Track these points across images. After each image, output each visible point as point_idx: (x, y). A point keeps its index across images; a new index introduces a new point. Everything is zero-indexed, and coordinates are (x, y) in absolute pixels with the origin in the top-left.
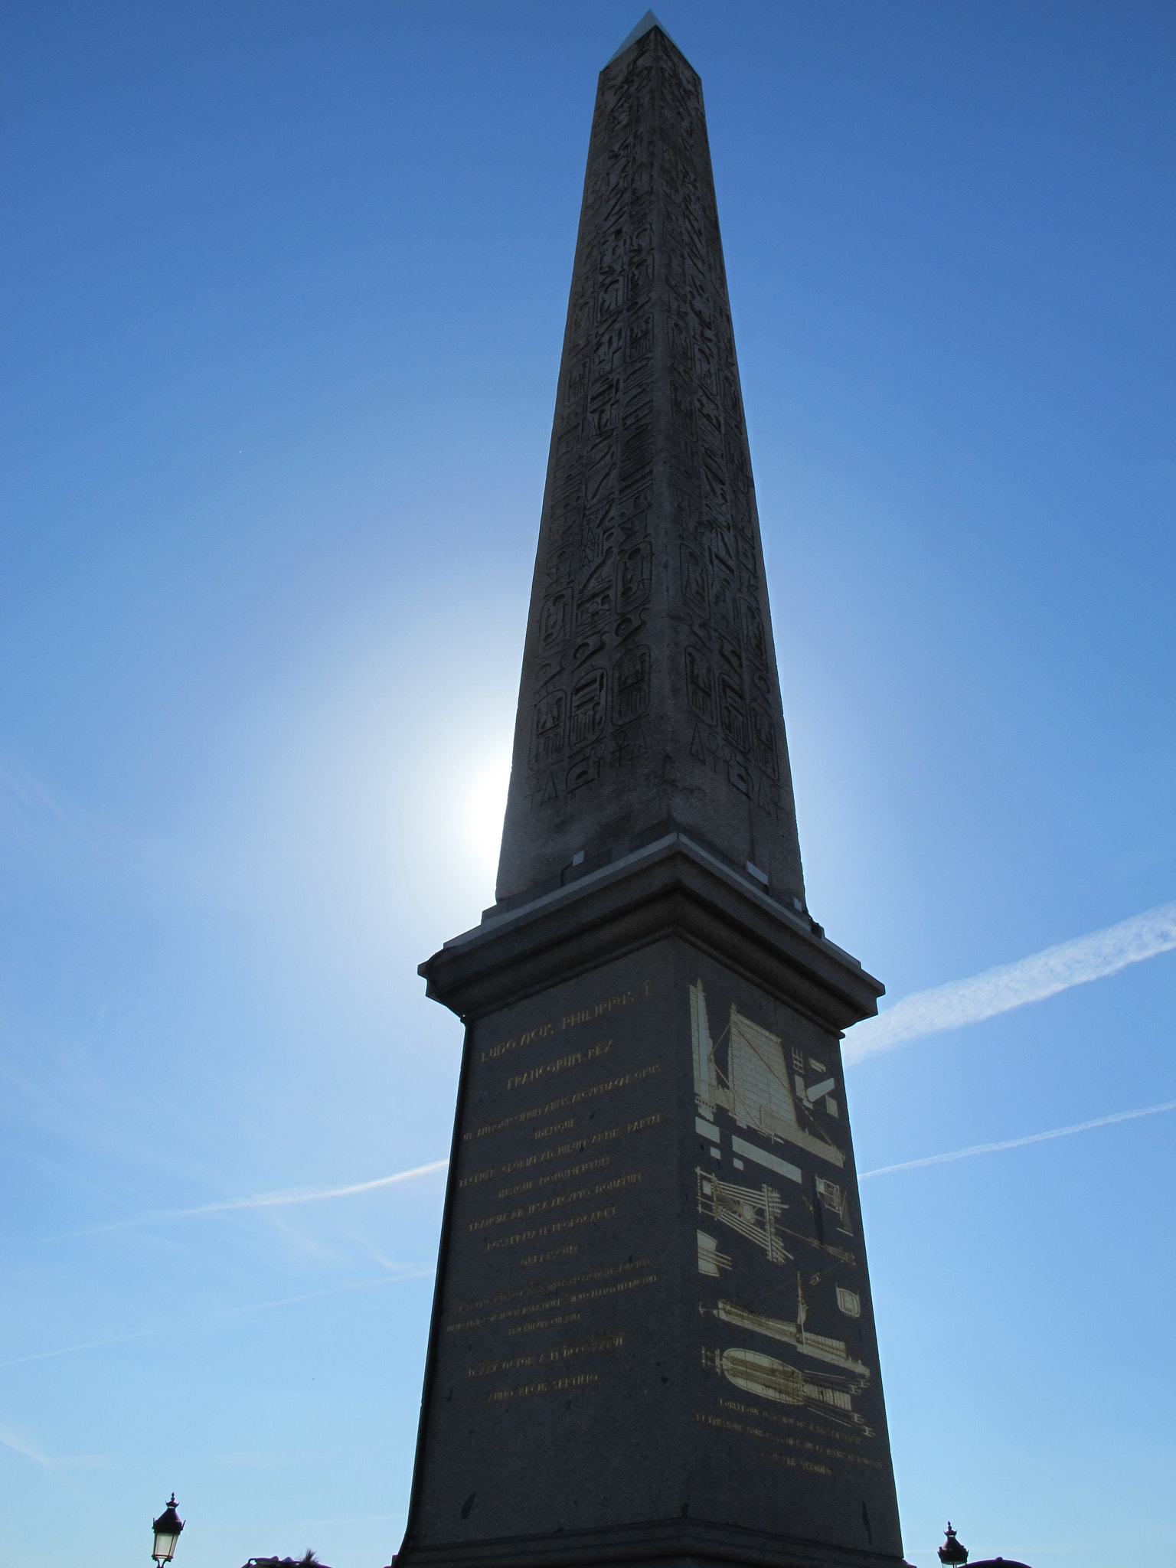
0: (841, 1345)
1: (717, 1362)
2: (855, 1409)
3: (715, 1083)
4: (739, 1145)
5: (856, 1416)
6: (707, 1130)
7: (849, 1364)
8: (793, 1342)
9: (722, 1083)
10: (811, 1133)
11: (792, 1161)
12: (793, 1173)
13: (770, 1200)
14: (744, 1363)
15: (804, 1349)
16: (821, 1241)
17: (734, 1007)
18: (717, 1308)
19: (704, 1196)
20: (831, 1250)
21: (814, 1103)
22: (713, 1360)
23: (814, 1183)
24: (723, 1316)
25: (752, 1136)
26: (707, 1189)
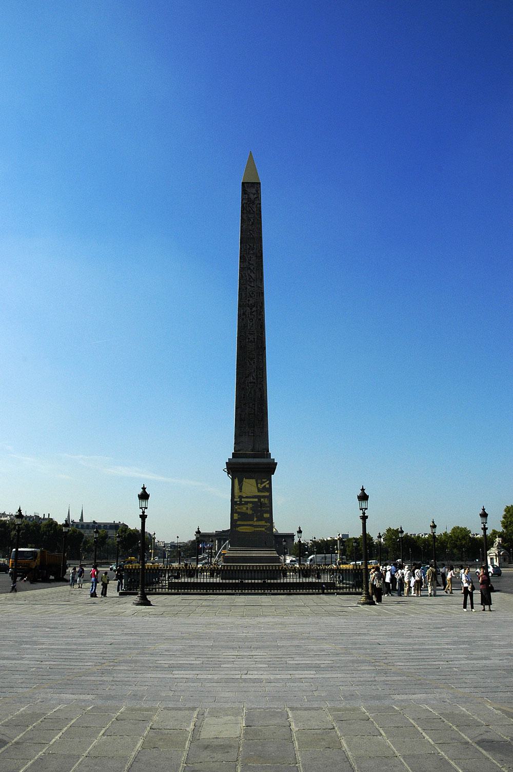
4: (243, 500)
7: (266, 524)
9: (241, 492)
12: (256, 500)
13: (250, 505)
15: (254, 524)
16: (261, 507)
25: (247, 497)
26: (236, 508)
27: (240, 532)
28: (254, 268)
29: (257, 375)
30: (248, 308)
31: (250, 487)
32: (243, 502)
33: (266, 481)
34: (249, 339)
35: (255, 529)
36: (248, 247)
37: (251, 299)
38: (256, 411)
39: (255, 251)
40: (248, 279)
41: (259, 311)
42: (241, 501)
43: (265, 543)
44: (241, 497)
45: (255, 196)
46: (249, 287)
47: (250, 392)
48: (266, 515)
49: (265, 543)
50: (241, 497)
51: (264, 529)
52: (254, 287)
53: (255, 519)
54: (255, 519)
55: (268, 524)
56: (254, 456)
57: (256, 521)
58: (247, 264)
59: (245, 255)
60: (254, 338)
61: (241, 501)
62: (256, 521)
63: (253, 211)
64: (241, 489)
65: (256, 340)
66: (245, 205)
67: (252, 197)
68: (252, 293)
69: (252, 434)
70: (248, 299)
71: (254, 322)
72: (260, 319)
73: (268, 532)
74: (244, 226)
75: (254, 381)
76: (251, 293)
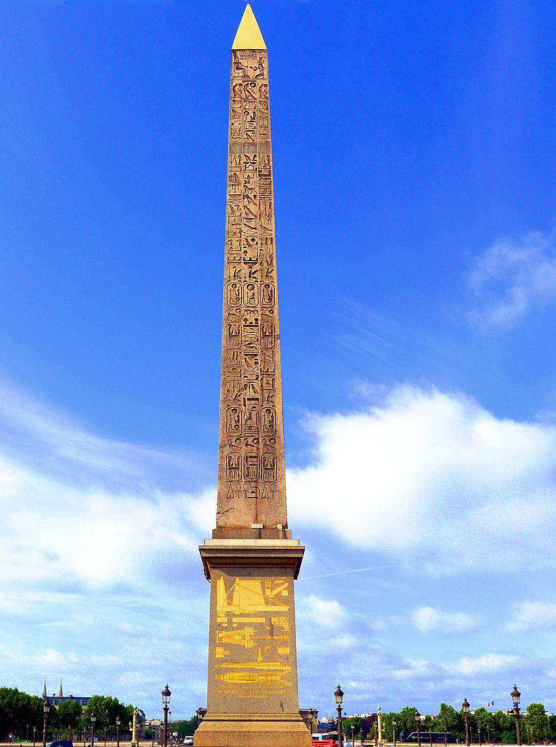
0: (279, 663)
1: (222, 678)
4: (235, 620)
5: (281, 681)
6: (222, 619)
8: (254, 667)
9: (229, 604)
12: (263, 620)
13: (249, 631)
16: (272, 635)
19: (219, 638)
20: (276, 637)
23: (271, 619)
24: (225, 666)
25: (242, 615)
26: (220, 635)
27: (227, 684)
28: (255, 196)
29: (262, 386)
30: (246, 266)
31: (250, 594)
32: (236, 625)
33: (282, 584)
34: (246, 320)
36: (244, 159)
37: (248, 249)
38: (261, 450)
39: (256, 166)
40: (244, 215)
41: (265, 271)
42: (230, 622)
43: (282, 706)
44: (229, 615)
45: (258, 72)
46: (245, 229)
47: (250, 418)
48: (283, 651)
49: (282, 706)
51: (278, 678)
52: (254, 228)
53: (260, 658)
54: (260, 658)
56: (259, 535)
58: (242, 187)
59: (238, 173)
60: (256, 320)
61: (230, 622)
62: (261, 662)
63: (255, 99)
64: (230, 598)
65: (260, 322)
66: (238, 87)
67: (252, 74)
68: (253, 240)
69: (254, 495)
70: (245, 249)
71: (256, 289)
72: (267, 286)
74: (236, 124)
75: (257, 396)
76: (249, 239)
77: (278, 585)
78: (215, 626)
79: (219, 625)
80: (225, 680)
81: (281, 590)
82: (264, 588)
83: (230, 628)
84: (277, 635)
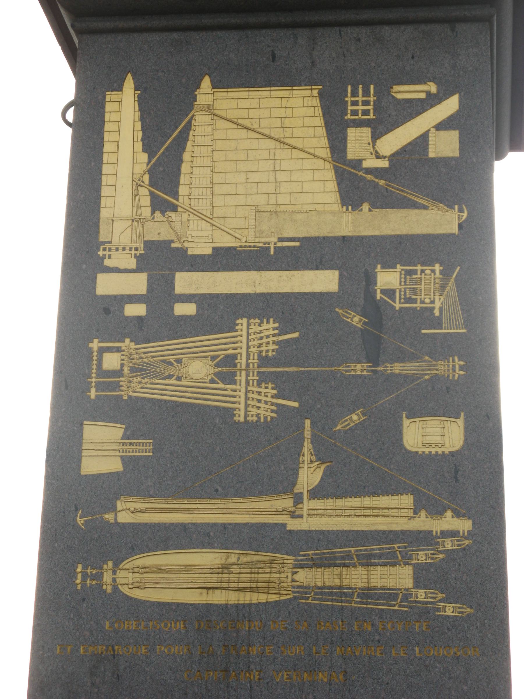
1: (107, 578)
2: (417, 584)
3: (147, 212)
4: (185, 282)
5: (421, 595)
6: (122, 282)
7: (423, 523)
10: (373, 206)
11: (319, 265)
12: (324, 281)
13: (254, 338)
14: (163, 569)
17: (206, 82)
18: (114, 509)
19: (102, 373)
20: (398, 368)
21: (394, 157)
22: (99, 577)
23: (370, 279)
24: (124, 518)
26: (111, 361)
33: (431, 101)
35: (304, 577)
42: (161, 294)
50: (161, 260)
53: (309, 475)
55: (449, 522)
57: (314, 494)
61: (161, 294)
62: (314, 494)
64: (164, 180)
73: (449, 610)
77: (414, 109)
78: (86, 317)
79: (107, 311)
80: (125, 590)
81: (429, 130)
82: (336, 129)
83: (160, 322)
84: (402, 357)
